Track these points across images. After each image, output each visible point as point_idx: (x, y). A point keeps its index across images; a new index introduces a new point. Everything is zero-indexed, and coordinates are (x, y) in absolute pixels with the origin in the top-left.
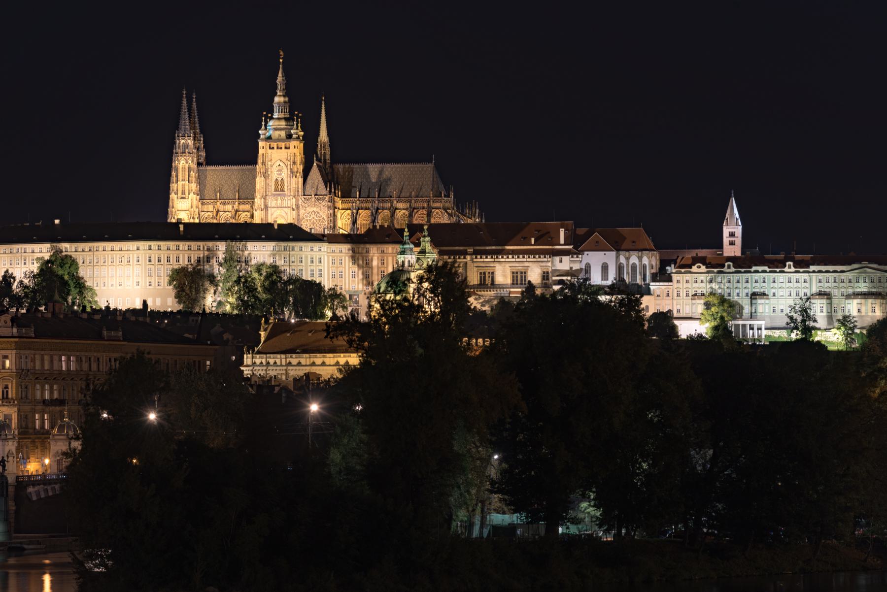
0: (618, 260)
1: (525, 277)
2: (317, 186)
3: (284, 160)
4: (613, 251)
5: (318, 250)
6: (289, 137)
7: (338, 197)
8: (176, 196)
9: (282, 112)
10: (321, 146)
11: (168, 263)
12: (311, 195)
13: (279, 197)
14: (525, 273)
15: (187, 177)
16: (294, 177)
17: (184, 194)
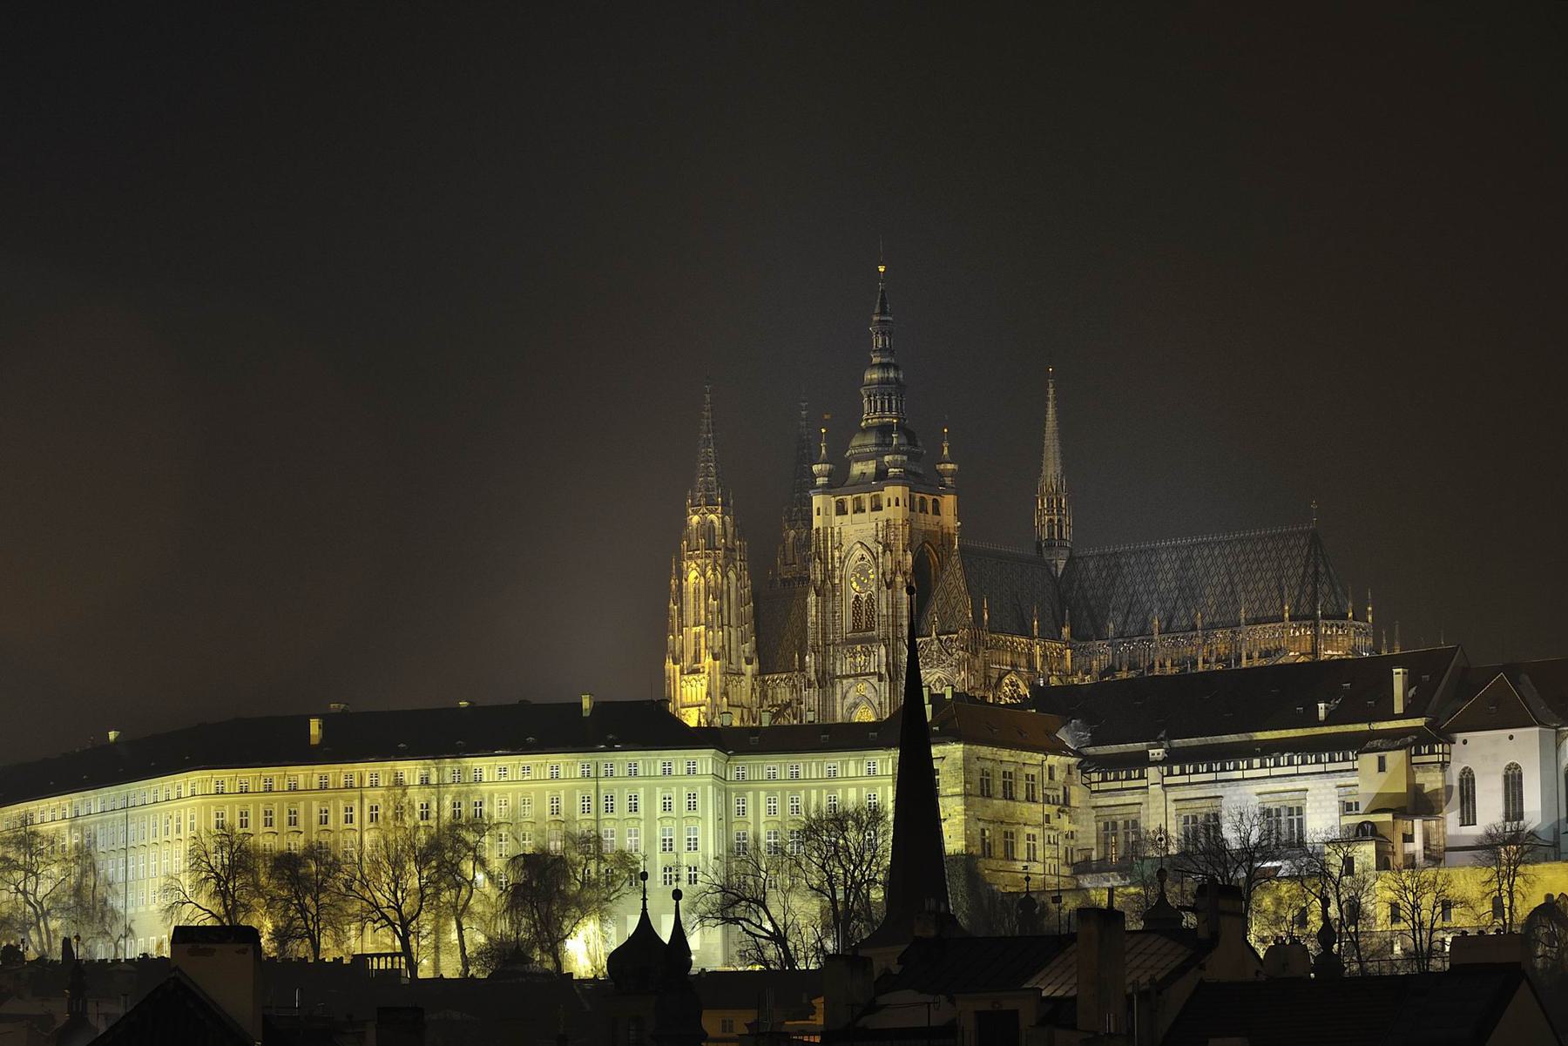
0: (1561, 754)
1: (1300, 822)
2: (954, 608)
3: (870, 543)
4: (1532, 725)
5: (685, 772)
6: (881, 475)
7: (1057, 637)
8: (678, 667)
9: (875, 411)
10: (1042, 501)
11: (269, 829)
12: (931, 635)
13: (859, 647)
14: (1300, 811)
15: (703, 612)
16: (885, 588)
17: (699, 663)
